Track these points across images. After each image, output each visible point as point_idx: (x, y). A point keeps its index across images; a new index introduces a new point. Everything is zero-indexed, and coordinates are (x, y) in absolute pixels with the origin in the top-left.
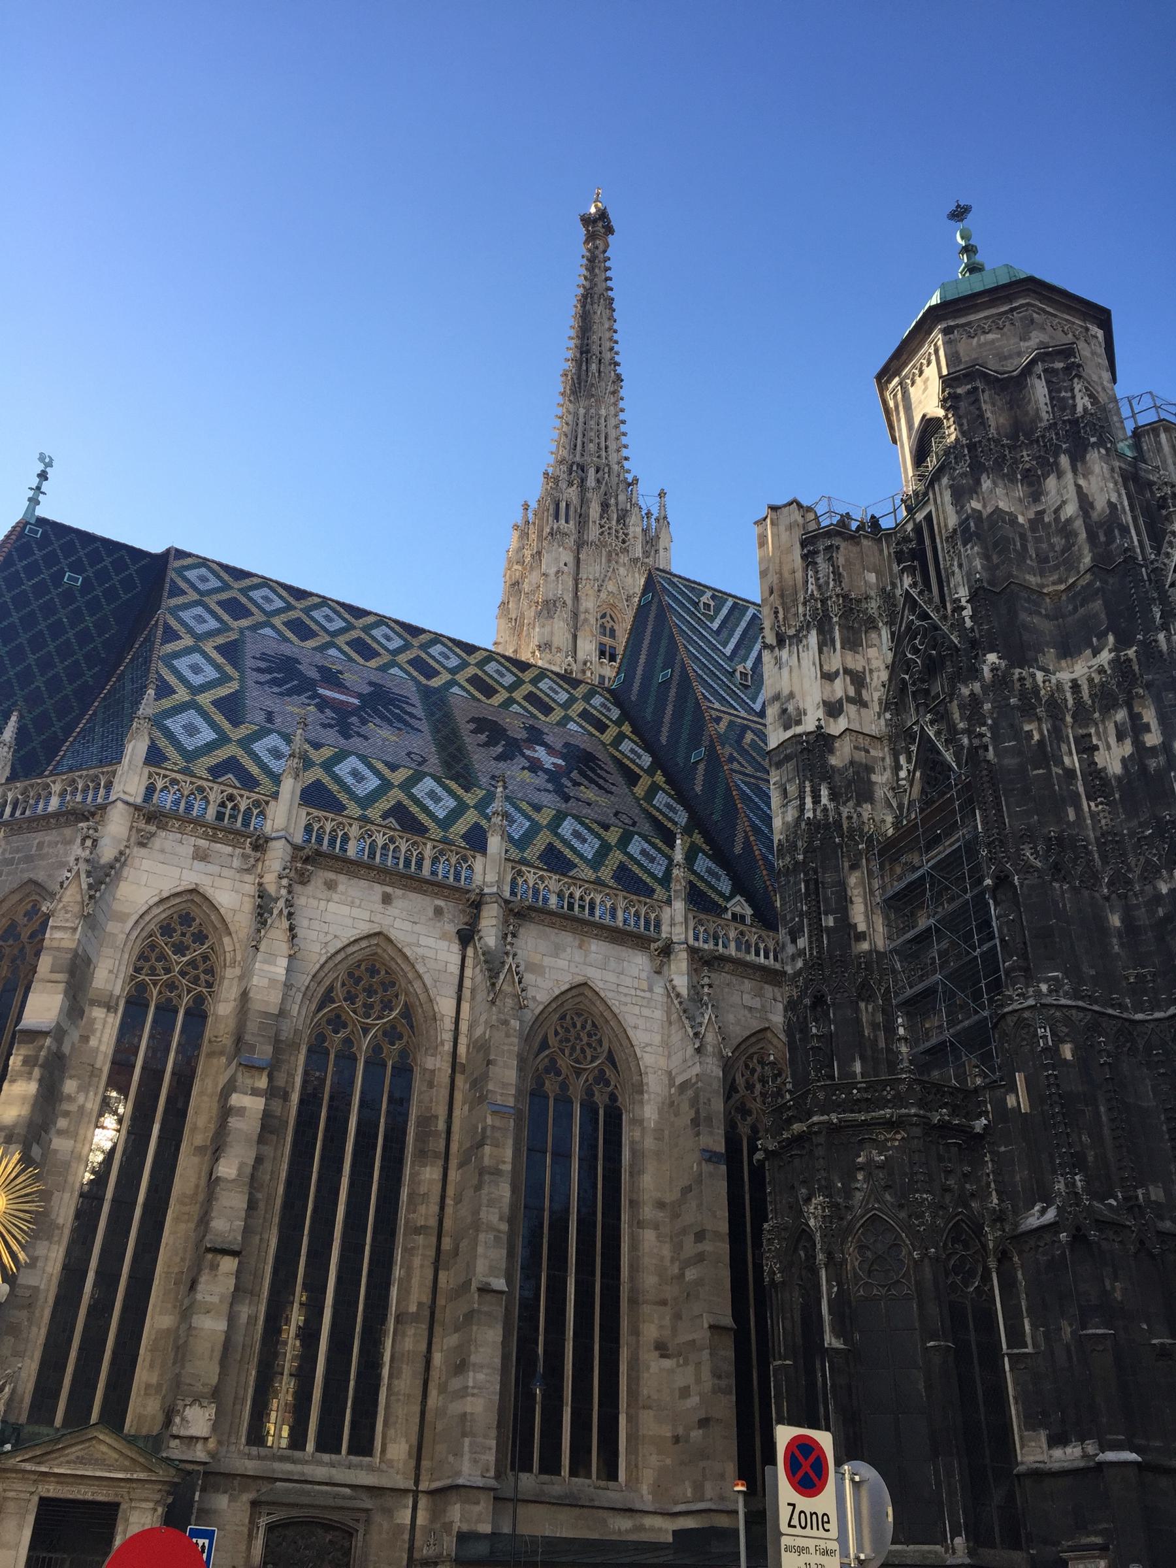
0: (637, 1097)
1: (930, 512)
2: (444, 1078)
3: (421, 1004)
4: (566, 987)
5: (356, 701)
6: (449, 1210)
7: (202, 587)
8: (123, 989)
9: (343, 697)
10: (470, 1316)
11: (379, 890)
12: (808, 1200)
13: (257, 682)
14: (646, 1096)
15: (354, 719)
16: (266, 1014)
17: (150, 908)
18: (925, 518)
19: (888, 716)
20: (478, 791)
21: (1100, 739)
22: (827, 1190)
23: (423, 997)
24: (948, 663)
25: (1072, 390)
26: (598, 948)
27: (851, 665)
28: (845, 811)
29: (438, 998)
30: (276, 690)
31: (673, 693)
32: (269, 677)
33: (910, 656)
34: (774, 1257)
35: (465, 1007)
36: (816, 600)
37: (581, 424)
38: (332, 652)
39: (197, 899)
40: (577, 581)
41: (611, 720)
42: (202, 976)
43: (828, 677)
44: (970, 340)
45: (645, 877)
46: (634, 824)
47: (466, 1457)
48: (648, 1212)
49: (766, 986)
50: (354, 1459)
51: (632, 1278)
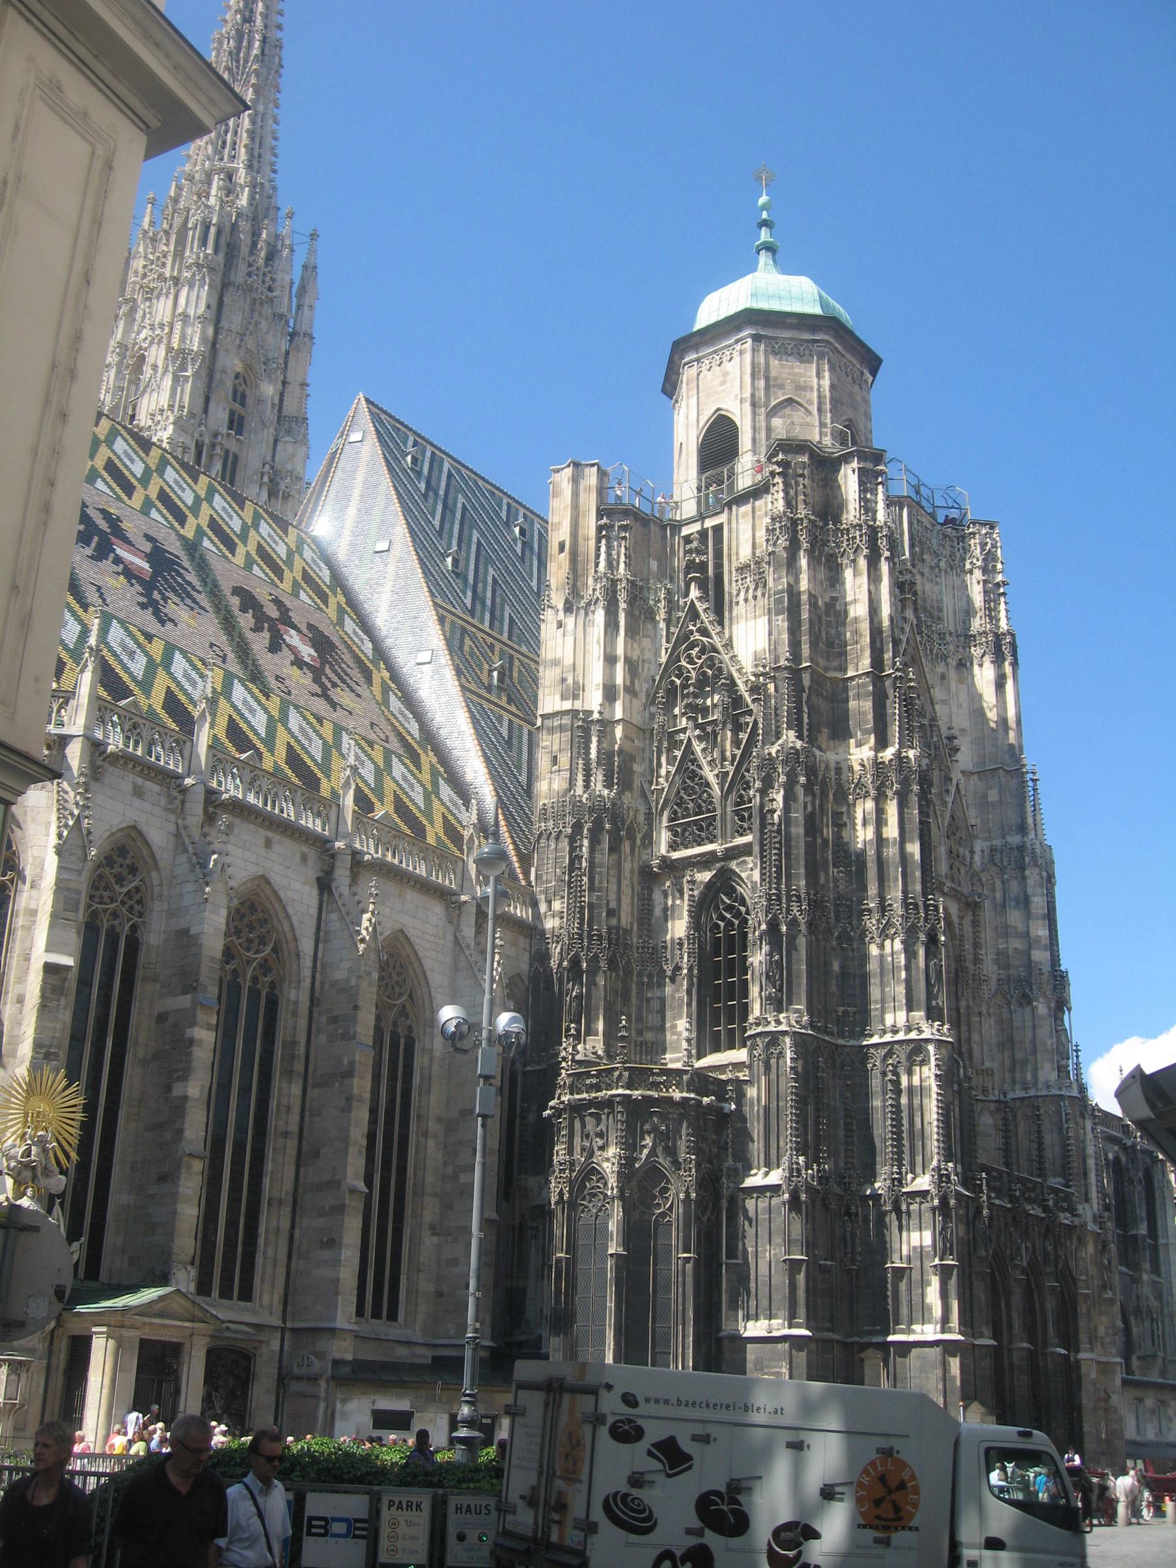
2: (304, 1009)
3: (287, 942)
5: (146, 566)
6: (307, 1120)
10: (340, 1209)
11: (263, 833)
12: (602, 1148)
23: (289, 935)
26: (412, 897)
27: (629, 655)
30: (89, 551)
35: (321, 946)
39: (133, 834)
43: (610, 660)
47: (339, 1309)
48: (433, 1126)
50: (243, 1304)
51: (415, 1175)
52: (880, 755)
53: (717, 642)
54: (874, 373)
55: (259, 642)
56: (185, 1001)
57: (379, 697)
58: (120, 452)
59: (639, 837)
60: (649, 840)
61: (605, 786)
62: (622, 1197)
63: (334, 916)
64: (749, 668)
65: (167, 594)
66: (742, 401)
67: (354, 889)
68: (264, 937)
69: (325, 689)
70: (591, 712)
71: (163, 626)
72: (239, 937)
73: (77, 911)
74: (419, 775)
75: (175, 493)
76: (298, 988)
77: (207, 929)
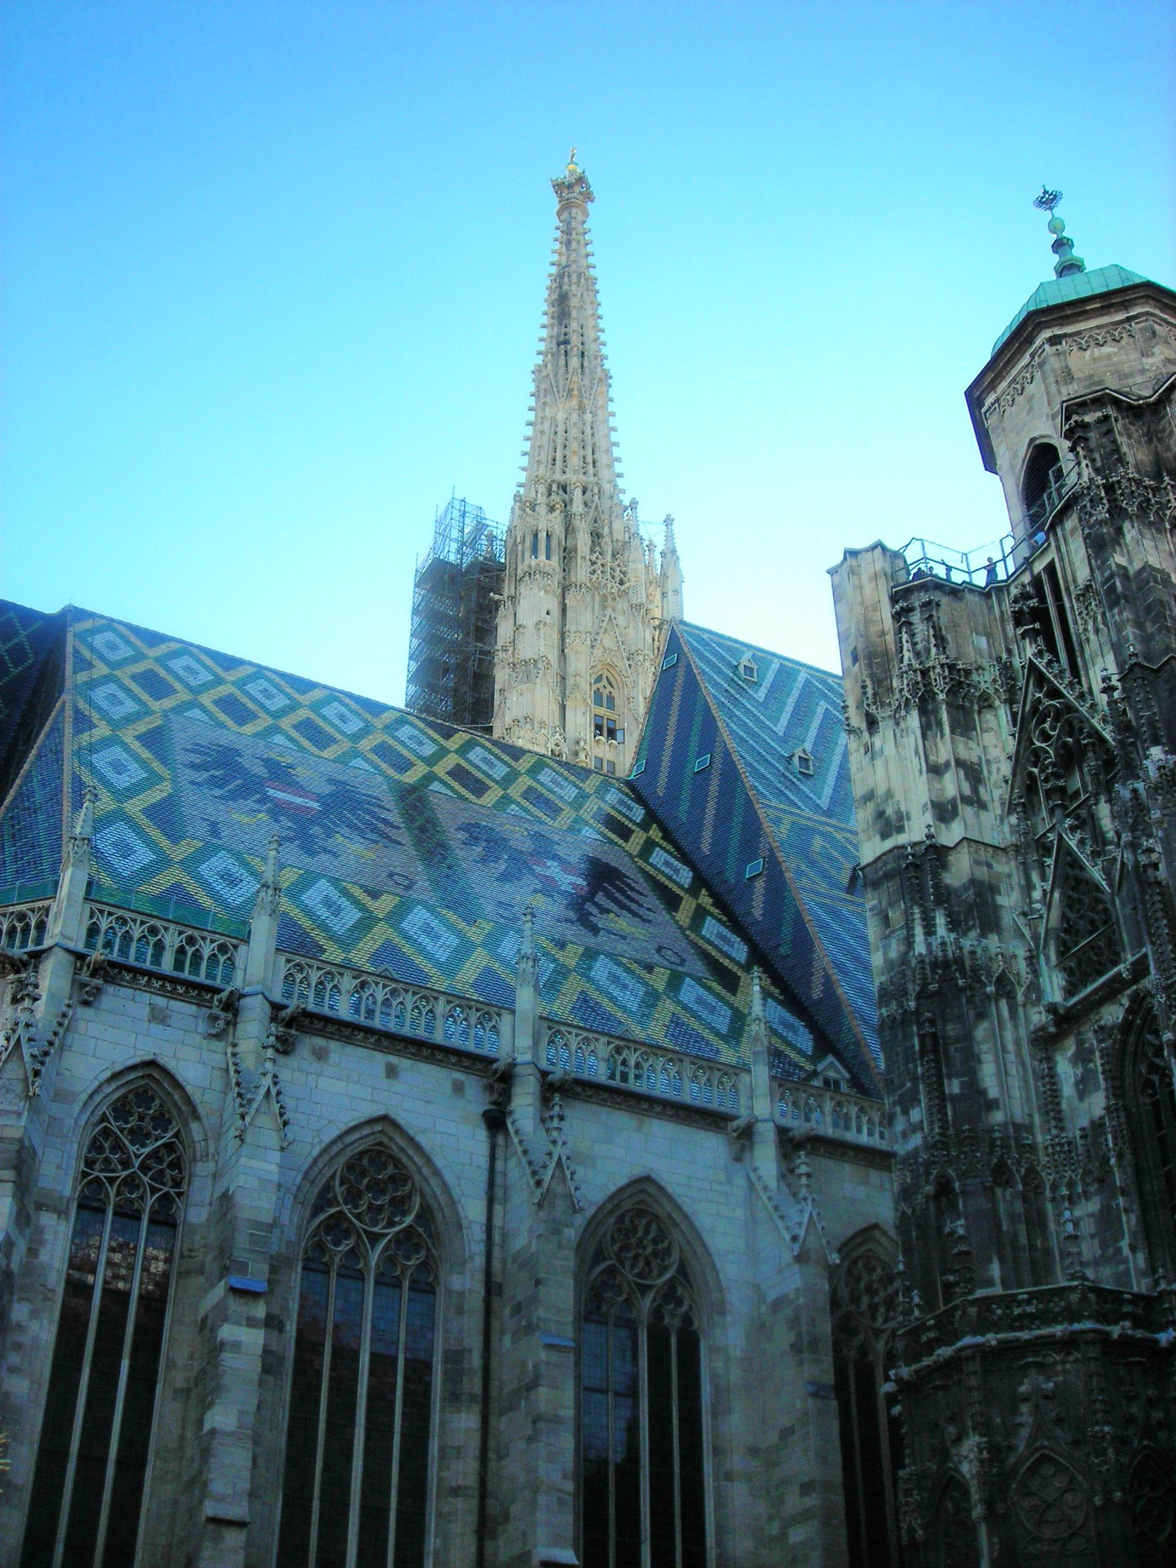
0: (717, 1319)
1: (1052, 563)
2: (475, 1301)
3: (441, 1209)
4: (625, 1181)
5: (316, 805)
6: (492, 1465)
7: (110, 656)
8: (74, 1190)
9: (299, 800)
11: (380, 1059)
12: (958, 1440)
13: (193, 783)
14: (729, 1318)
15: (316, 830)
16: (257, 1224)
17: (100, 1087)
18: (1045, 569)
19: (1013, 819)
20: (484, 925)
22: (984, 1428)
23: (441, 1198)
24: (1090, 754)
26: (662, 1130)
27: (964, 755)
29: (463, 1200)
30: (217, 792)
31: (714, 788)
32: (206, 775)
33: (1038, 744)
34: (913, 1511)
35: (498, 1209)
36: (915, 671)
37: (560, 432)
38: (278, 739)
39: (156, 1074)
40: (563, 635)
41: (634, 823)
42: (168, 1171)
43: (935, 770)
44: (1082, 353)
45: (706, 1034)
46: (683, 962)
48: (736, 1461)
51: (719, 1543)
53: (1070, 696)
60: (1035, 988)
61: (950, 930)
62: (992, 1516)
63: (512, 1163)
66: (1053, 417)
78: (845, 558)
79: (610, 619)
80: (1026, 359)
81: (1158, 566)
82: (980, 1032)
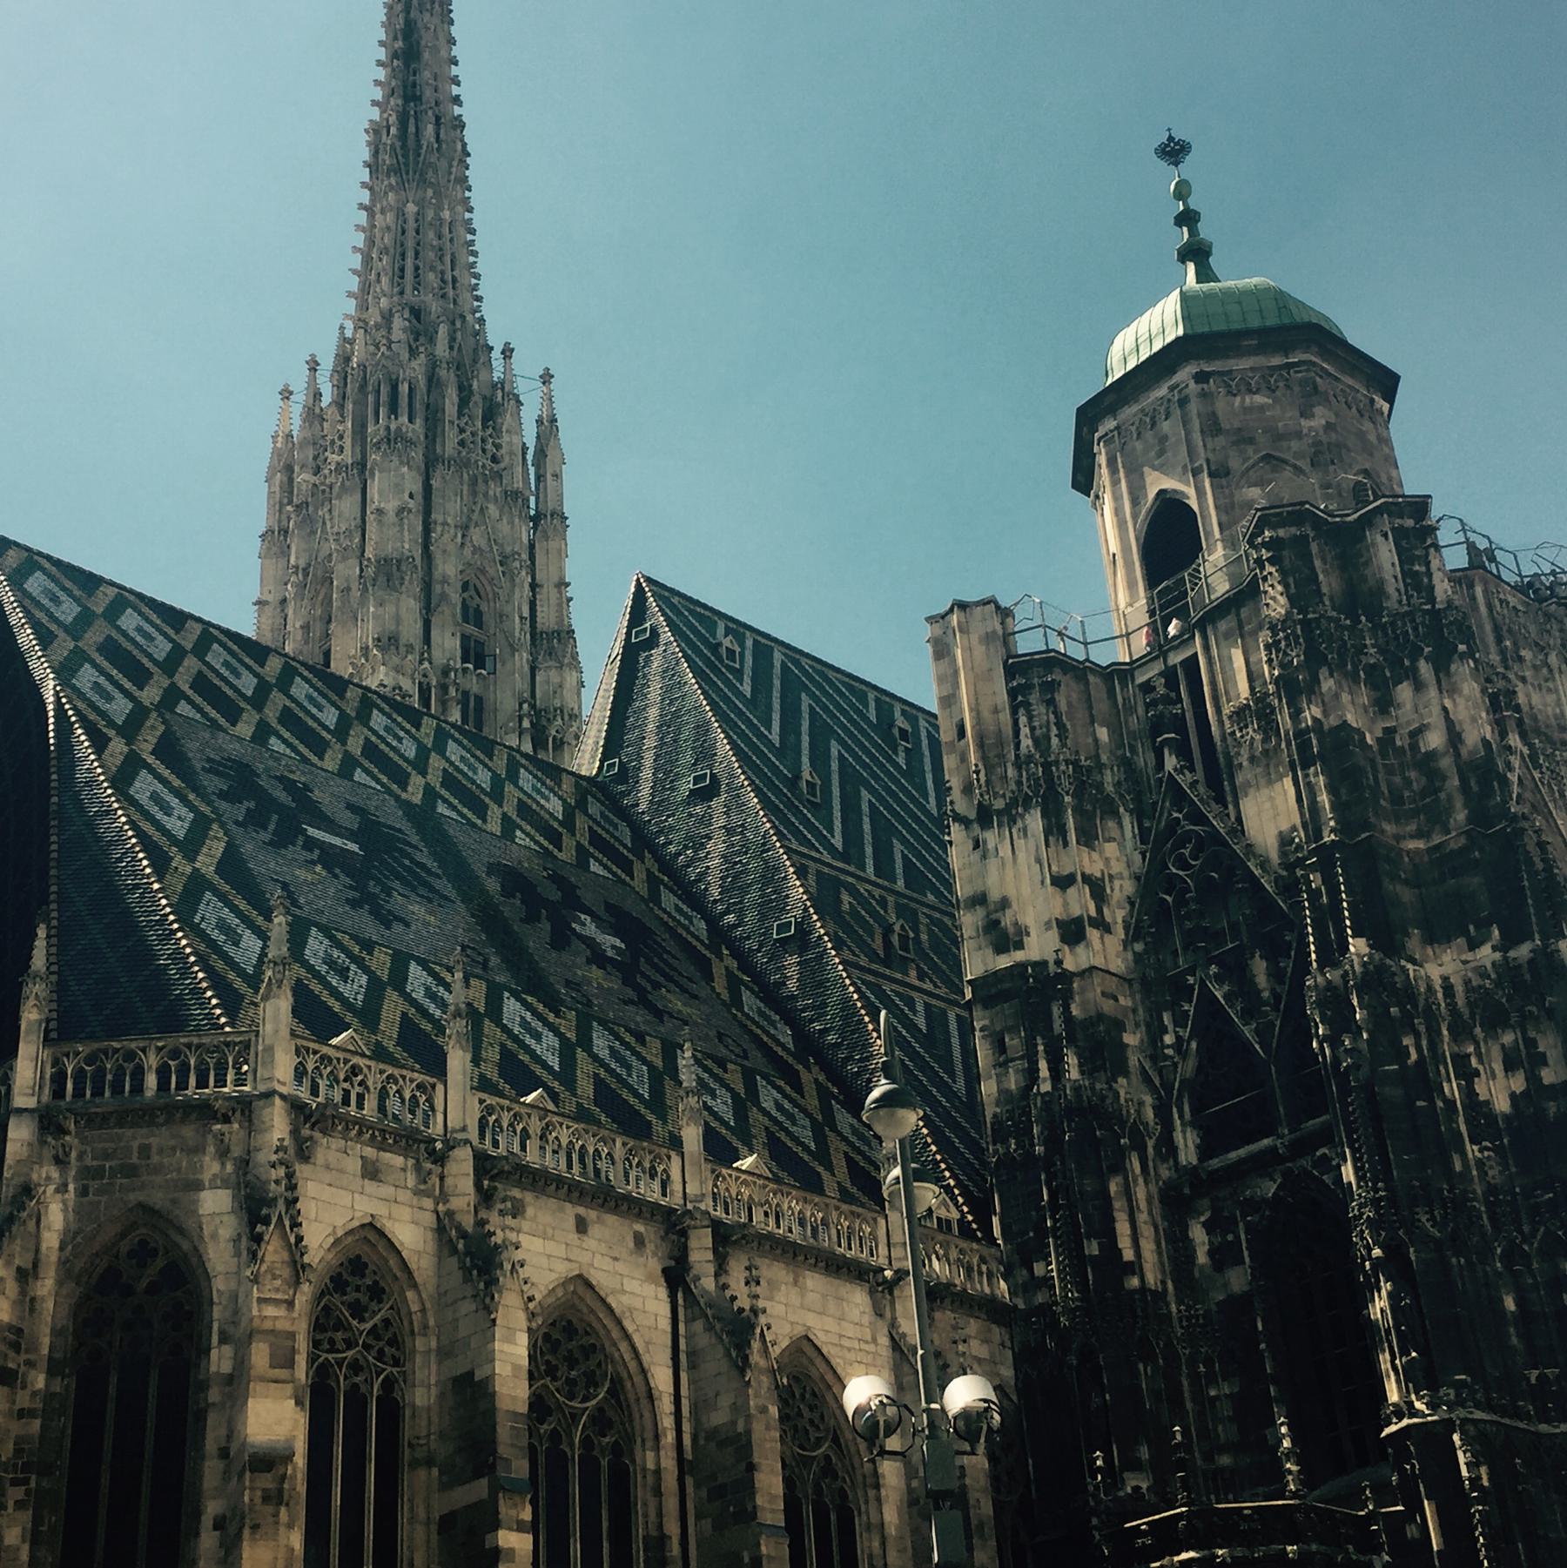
3: (630, 1377)
9: (337, 841)
11: (571, 1211)
18: (1181, 663)
21: (1481, 1061)
23: (632, 1365)
25: (1428, 564)
27: (1088, 871)
28: (1098, 1086)
30: (265, 836)
33: (1174, 871)
35: (684, 1376)
39: (372, 1236)
41: (625, 846)
43: (1063, 882)
49: (994, 1327)
52: (1512, 954)
54: (1390, 397)
55: (536, 939)
56: (480, 1488)
57: (725, 996)
58: (302, 698)
59: (1150, 1144)
64: (1274, 856)
65: (390, 883)
67: (723, 1280)
68: (593, 1372)
69: (641, 992)
70: (1044, 963)
71: (388, 928)
72: (554, 1379)
73: (290, 1364)
74: (801, 1102)
75: (388, 744)
76: (657, 1449)
77: (502, 1369)
78: (951, 610)
79: (482, 509)
80: (1162, 391)
81: (1355, 725)
82: (1113, 1188)
